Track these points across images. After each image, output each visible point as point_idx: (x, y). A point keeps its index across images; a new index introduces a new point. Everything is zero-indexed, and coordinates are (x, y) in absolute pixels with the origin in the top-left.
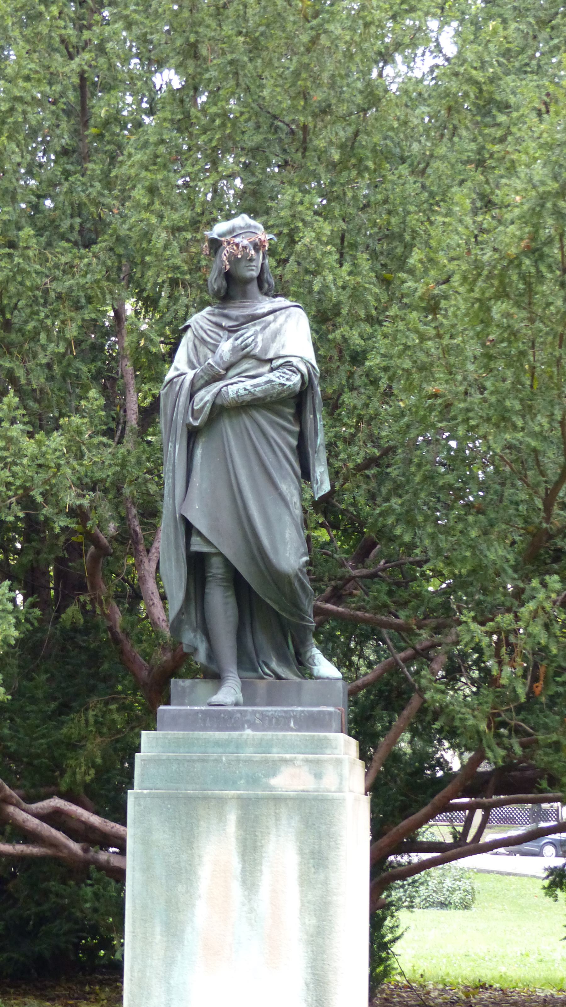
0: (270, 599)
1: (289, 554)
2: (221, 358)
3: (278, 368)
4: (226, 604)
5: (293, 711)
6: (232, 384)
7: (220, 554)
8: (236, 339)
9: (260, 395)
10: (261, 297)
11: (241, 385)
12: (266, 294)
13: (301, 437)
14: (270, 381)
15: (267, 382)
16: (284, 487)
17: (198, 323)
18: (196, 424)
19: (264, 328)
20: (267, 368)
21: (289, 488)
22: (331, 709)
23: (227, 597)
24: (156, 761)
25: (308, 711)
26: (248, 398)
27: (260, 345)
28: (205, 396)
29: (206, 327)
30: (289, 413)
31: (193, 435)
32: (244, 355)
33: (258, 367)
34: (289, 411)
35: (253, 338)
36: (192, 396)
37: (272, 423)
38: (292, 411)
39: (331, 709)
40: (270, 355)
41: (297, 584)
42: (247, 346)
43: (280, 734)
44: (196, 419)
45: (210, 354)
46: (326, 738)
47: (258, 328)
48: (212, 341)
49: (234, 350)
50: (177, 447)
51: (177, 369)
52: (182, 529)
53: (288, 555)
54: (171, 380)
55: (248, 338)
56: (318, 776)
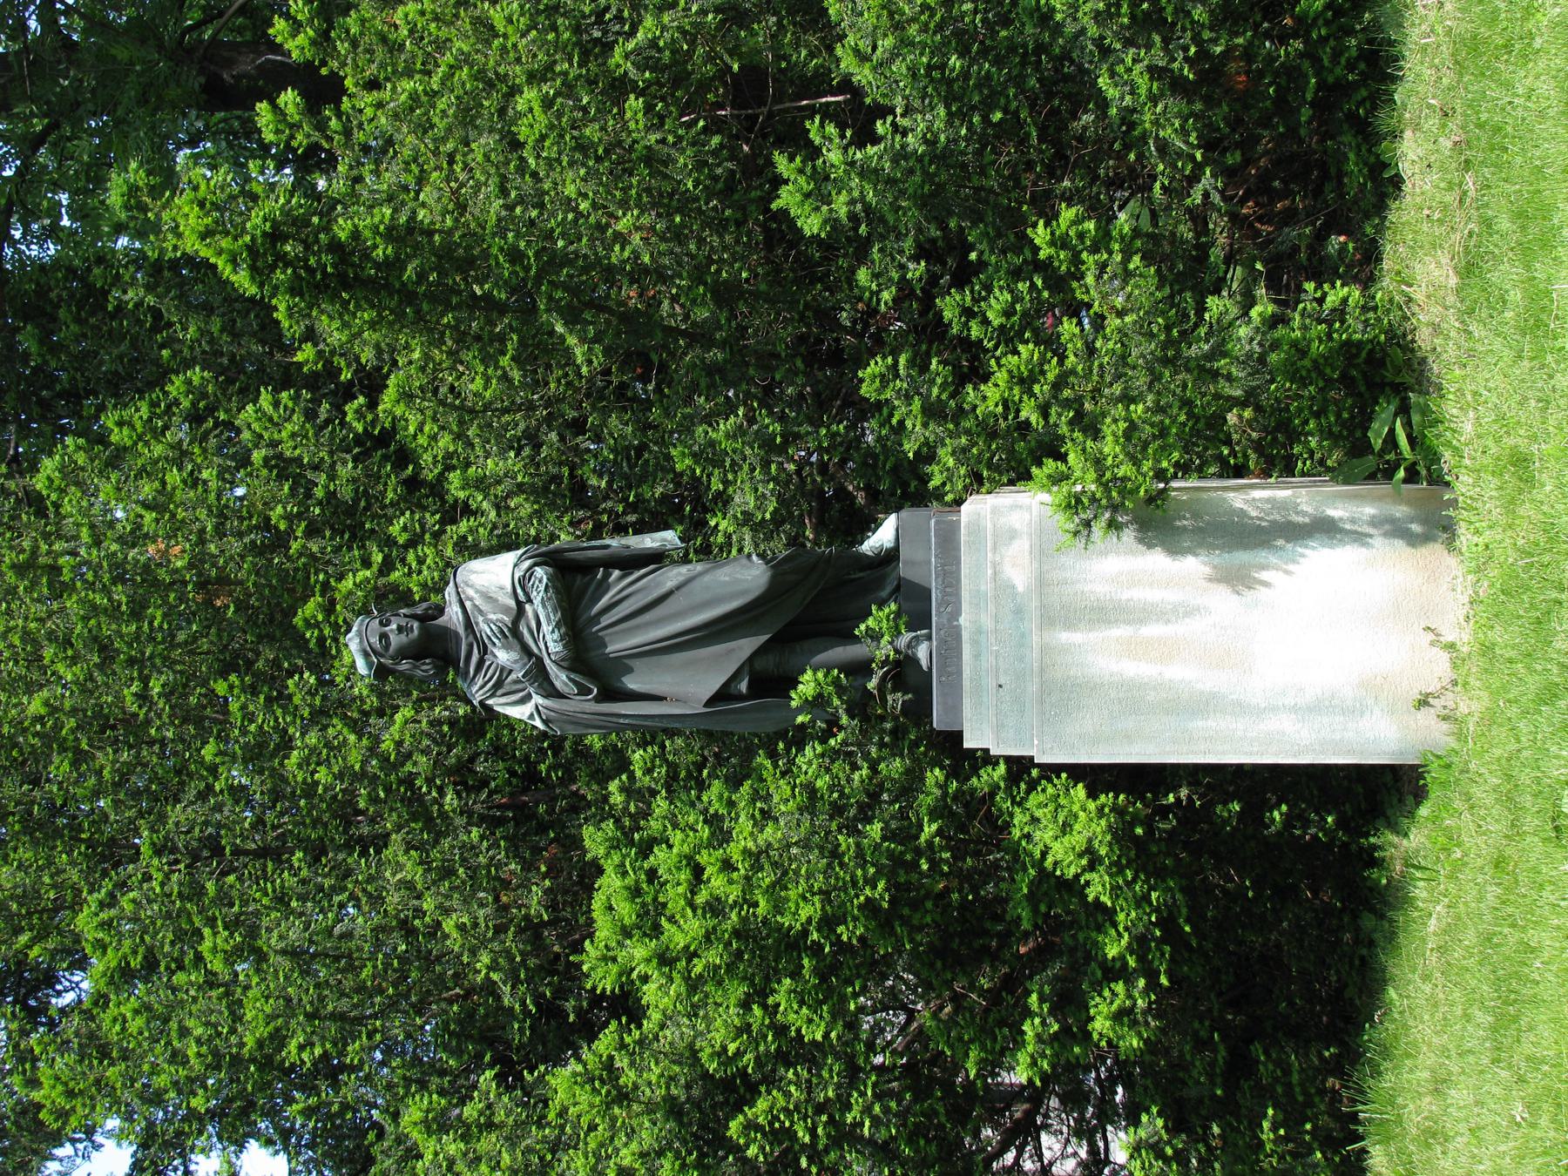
2: (516, 662)
3: (527, 595)
11: (548, 638)
15: (544, 606)
16: (670, 585)
19: (480, 612)
20: (527, 607)
21: (672, 576)
22: (933, 522)
24: (999, 728)
27: (500, 616)
28: (560, 678)
32: (513, 634)
34: (579, 580)
36: (561, 696)
38: (579, 577)
39: (933, 522)
40: (512, 603)
42: (502, 632)
45: (513, 676)
46: (968, 526)
47: (480, 619)
49: (507, 647)
51: (531, 717)
54: (545, 722)
56: (1013, 535)
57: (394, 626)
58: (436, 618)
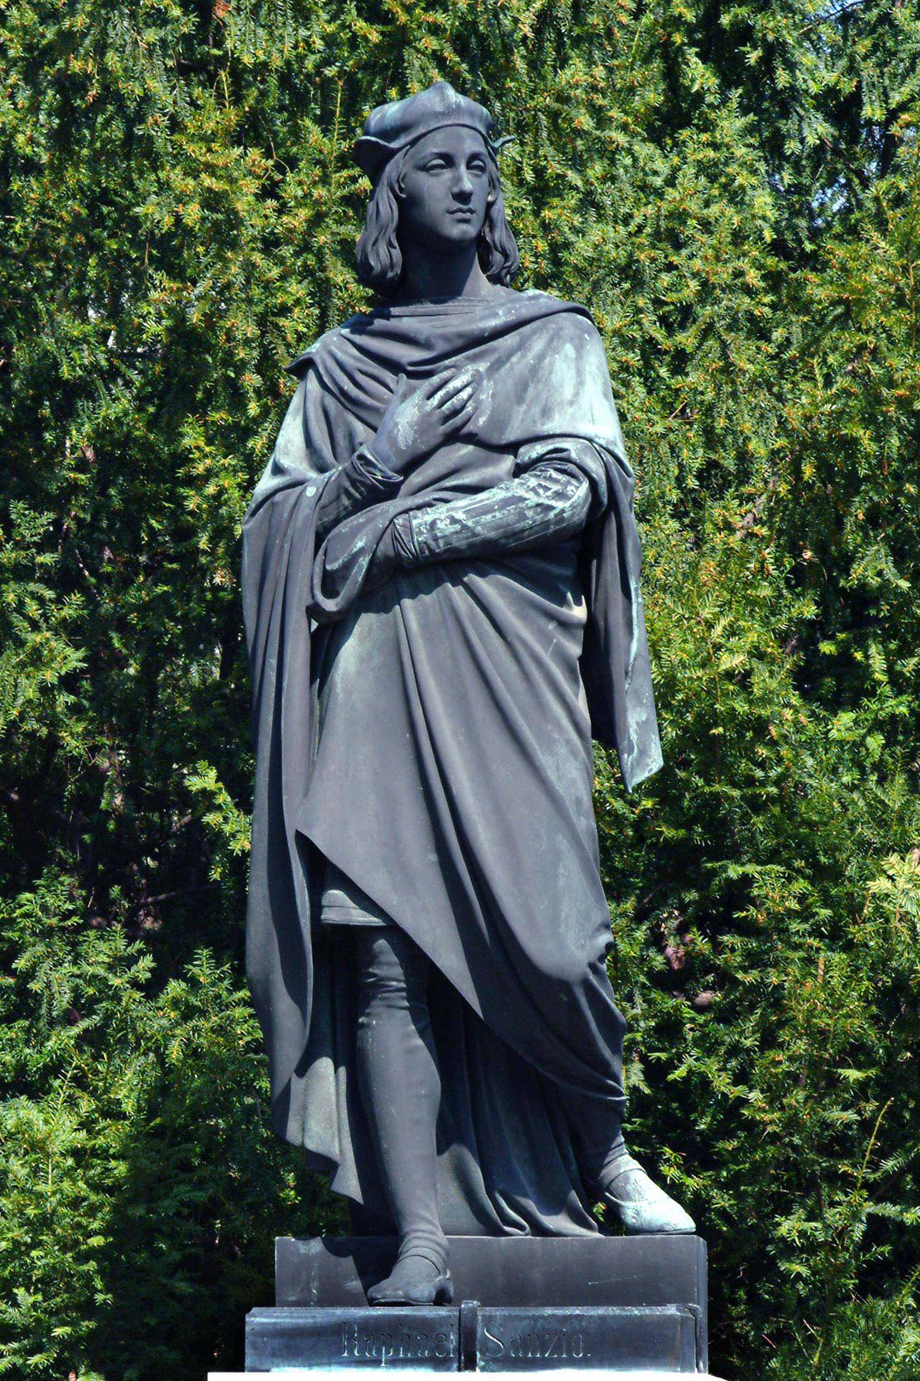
2: (393, 441)
6: (419, 508)
8: (430, 396)
15: (506, 503)
19: (497, 365)
20: (507, 463)
33: (485, 463)
40: (511, 435)
55: (459, 391)
57: (468, 184)
58: (485, 267)
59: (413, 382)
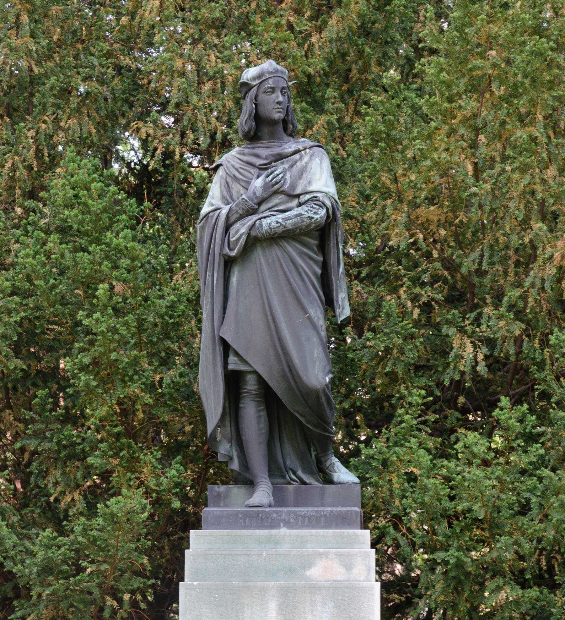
0: (298, 413)
1: (317, 372)
2: (254, 193)
4: (260, 417)
5: (323, 511)
6: (265, 217)
7: (255, 372)
8: (267, 177)
9: (290, 227)
10: (286, 138)
11: (273, 218)
12: (291, 135)
13: (325, 266)
14: (300, 215)
15: (297, 216)
17: (229, 162)
18: (233, 254)
19: (292, 166)
20: (295, 202)
21: (316, 313)
23: (260, 411)
25: (336, 511)
26: (280, 230)
27: (288, 182)
29: (237, 166)
30: (314, 244)
31: (229, 264)
32: (273, 191)
33: (288, 202)
34: (314, 242)
35: (282, 175)
36: (227, 228)
37: (301, 254)
40: (298, 191)
41: (323, 399)
42: (277, 183)
43: (314, 532)
44: (231, 250)
45: (242, 191)
47: (286, 166)
48: (245, 179)
49: (266, 186)
50: (215, 275)
51: (213, 205)
52: (219, 350)
53: (316, 372)
55: (278, 175)
59: (261, 172)
